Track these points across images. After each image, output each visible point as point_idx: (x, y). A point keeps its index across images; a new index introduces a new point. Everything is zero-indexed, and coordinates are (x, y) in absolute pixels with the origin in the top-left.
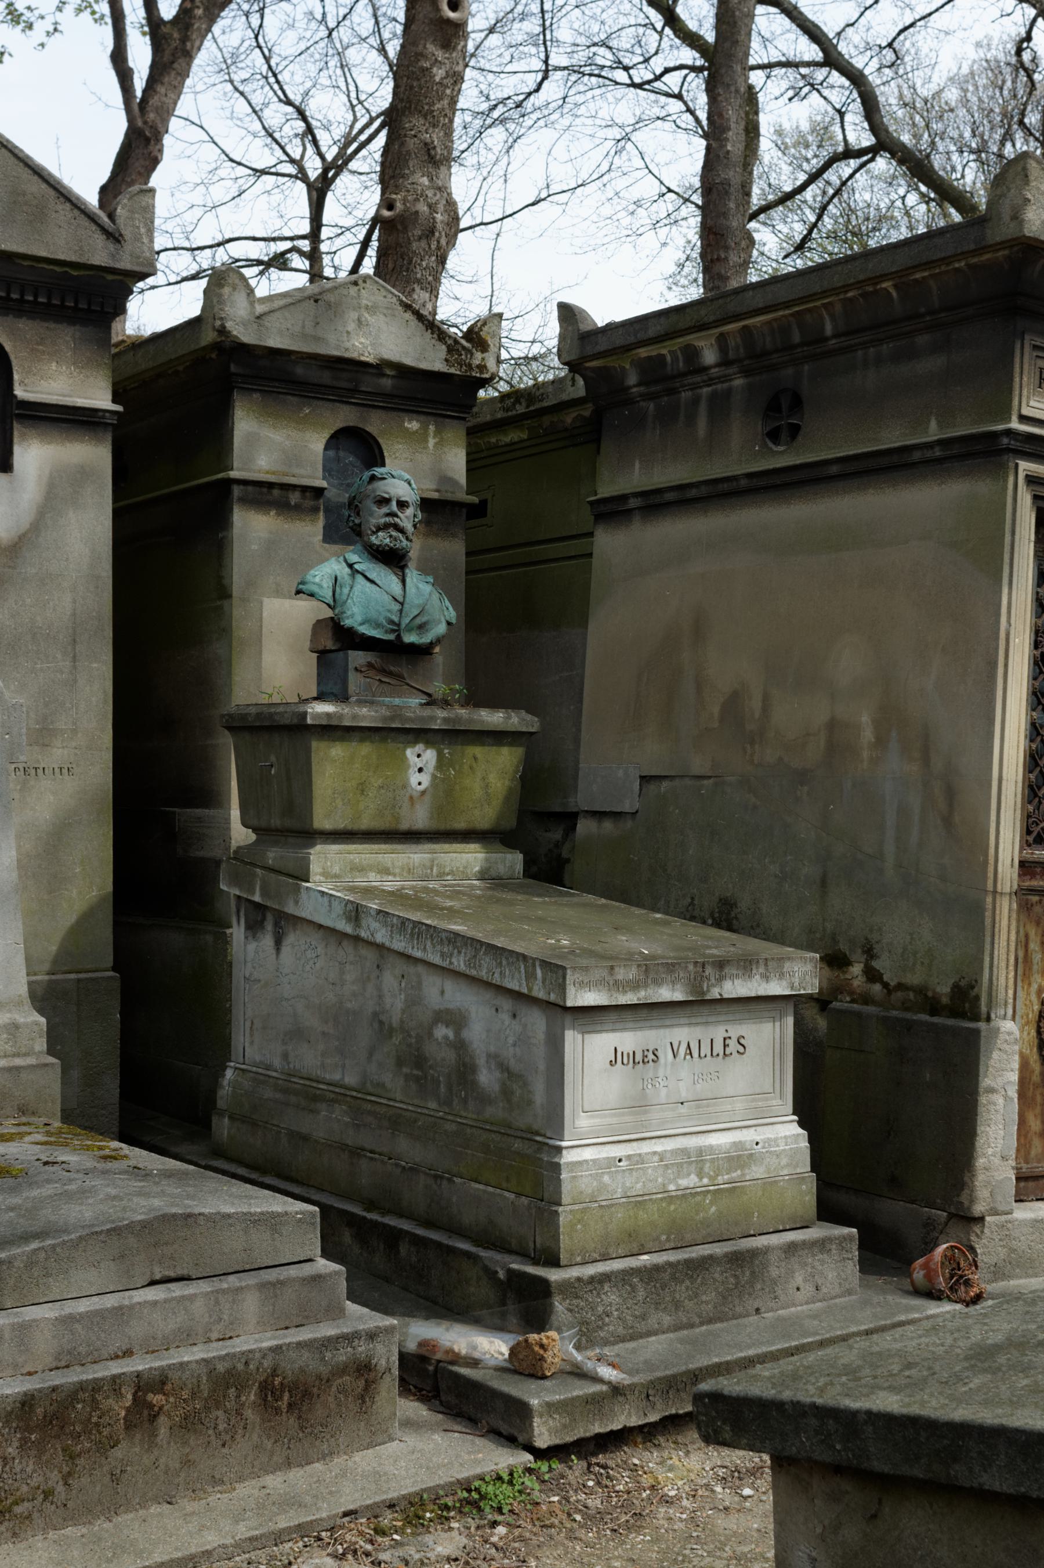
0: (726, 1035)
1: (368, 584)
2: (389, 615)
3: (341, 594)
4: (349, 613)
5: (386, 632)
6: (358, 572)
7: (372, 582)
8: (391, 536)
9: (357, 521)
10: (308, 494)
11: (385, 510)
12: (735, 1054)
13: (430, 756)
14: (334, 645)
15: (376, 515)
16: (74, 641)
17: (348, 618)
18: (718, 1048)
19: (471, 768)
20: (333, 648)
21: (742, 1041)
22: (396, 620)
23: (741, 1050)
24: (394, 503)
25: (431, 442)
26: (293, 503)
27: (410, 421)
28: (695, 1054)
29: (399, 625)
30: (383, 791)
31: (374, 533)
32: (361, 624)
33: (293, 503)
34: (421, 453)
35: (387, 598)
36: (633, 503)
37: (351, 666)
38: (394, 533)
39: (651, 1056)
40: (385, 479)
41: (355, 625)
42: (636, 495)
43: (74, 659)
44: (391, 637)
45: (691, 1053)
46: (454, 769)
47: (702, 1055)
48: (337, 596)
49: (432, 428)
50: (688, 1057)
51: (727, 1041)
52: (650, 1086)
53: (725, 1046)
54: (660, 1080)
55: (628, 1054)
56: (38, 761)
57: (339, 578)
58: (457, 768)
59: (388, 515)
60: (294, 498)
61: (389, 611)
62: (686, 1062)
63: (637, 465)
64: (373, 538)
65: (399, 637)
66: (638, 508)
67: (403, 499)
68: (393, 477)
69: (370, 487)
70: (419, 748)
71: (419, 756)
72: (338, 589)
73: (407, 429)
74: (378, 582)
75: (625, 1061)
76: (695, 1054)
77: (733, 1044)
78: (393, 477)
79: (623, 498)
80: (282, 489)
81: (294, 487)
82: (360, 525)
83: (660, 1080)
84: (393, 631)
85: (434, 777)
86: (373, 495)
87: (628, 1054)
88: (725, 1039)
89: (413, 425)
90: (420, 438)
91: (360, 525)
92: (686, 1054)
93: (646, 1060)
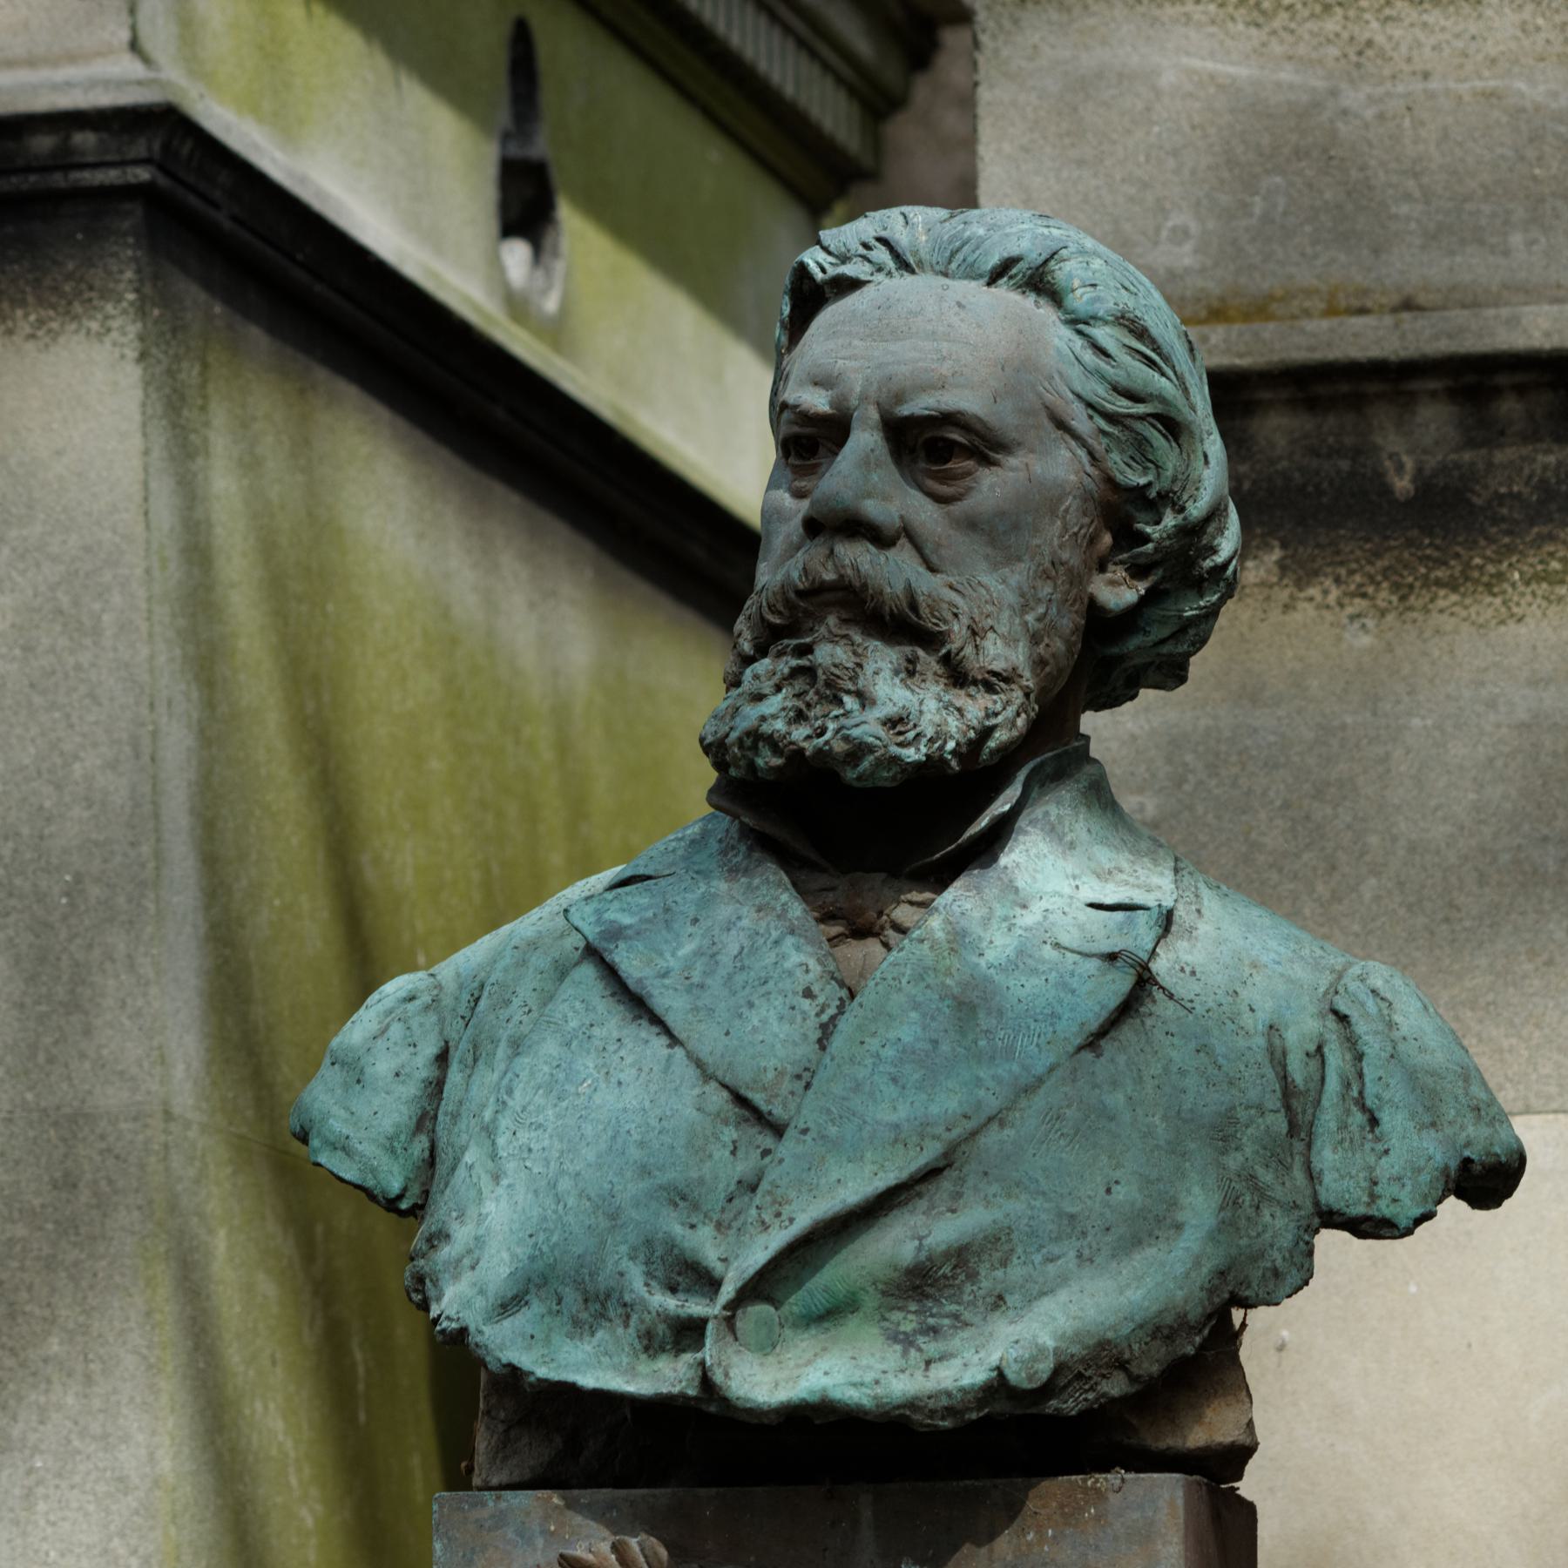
2: (674, 1226)
4: (462, 1235)
5: (651, 1344)
7: (637, 1004)
10: (1509, 407)
24: (865, 439)
26: (1403, 485)
32: (508, 1306)
33: (1403, 485)
40: (853, 284)
41: (472, 1319)
60: (1411, 446)
61: (681, 1197)
67: (920, 405)
68: (904, 265)
80: (1312, 405)
81: (1394, 379)
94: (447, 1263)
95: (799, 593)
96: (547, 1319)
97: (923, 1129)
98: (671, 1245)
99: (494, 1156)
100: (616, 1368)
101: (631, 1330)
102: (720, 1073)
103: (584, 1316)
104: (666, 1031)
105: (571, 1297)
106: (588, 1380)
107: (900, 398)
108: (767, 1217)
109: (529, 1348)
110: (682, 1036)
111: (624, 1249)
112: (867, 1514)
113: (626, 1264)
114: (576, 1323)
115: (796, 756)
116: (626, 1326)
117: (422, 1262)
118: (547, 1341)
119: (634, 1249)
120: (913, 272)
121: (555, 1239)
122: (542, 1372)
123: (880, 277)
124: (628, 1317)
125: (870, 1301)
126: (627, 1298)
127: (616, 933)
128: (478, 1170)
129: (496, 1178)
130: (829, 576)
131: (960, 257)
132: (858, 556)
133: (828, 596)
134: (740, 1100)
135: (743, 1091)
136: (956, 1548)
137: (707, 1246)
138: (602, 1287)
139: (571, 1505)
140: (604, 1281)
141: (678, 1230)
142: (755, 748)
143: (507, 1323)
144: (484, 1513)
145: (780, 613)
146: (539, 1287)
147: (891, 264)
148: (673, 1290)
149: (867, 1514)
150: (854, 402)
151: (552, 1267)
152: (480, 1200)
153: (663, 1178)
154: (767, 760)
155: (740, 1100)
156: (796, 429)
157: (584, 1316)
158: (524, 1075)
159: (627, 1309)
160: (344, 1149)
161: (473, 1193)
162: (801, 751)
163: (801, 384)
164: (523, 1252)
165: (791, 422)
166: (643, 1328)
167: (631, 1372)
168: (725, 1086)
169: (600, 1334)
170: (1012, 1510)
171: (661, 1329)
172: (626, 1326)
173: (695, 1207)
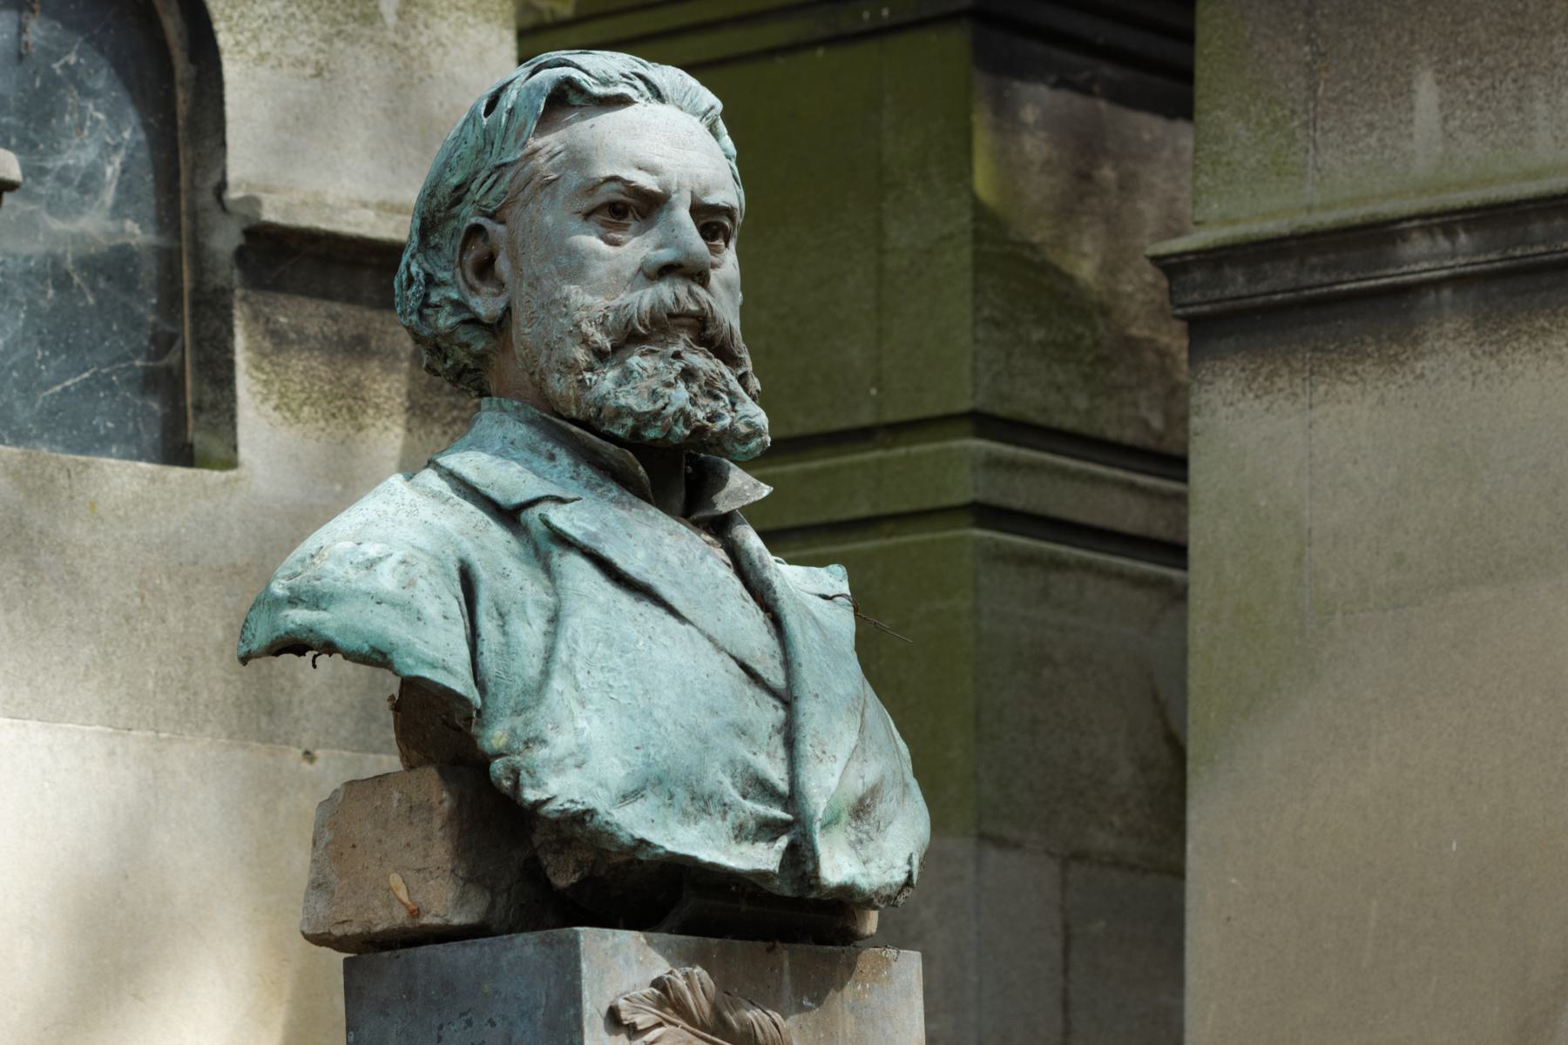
1: (624, 601)
2: (742, 750)
3: (508, 649)
4: (561, 743)
6: (563, 540)
8: (688, 375)
9: (485, 305)
11: (638, 248)
14: (461, 901)
15: (599, 270)
17: (558, 766)
20: (457, 920)
22: (777, 775)
24: (683, 214)
29: (792, 799)
31: (601, 355)
32: (628, 797)
34: (352, 39)
36: (1421, 257)
37: (593, 1008)
38: (701, 361)
40: (622, 101)
42: (1445, 221)
44: (764, 857)
48: (489, 661)
57: (483, 574)
59: (666, 271)
63: (1426, 91)
64: (606, 381)
65: (800, 857)
66: (1458, 281)
68: (658, 95)
69: (551, 141)
72: (487, 625)
74: (667, 592)
78: (658, 95)
79: (1376, 235)
82: (499, 327)
84: (768, 830)
86: (574, 179)
91: (499, 327)
94: (547, 762)
95: (671, 315)
96: (662, 809)
98: (748, 766)
99: (577, 688)
100: (718, 848)
101: (728, 823)
102: (727, 647)
103: (691, 809)
104: (672, 611)
105: (682, 795)
106: (706, 855)
107: (706, 192)
108: (819, 753)
109: (652, 829)
110: (690, 618)
111: (717, 764)
112: (786, 964)
113: (721, 776)
114: (685, 814)
115: (700, 431)
116: (724, 819)
117: (518, 758)
118: (665, 826)
119: (724, 765)
120: (663, 102)
121: (665, 752)
122: (670, 847)
123: (642, 101)
124: (725, 813)
125: (845, 817)
126: (727, 800)
127: (595, 537)
128: (567, 696)
129: (582, 704)
130: (693, 307)
131: (688, 98)
133: (685, 321)
134: (744, 667)
135: (748, 662)
136: (827, 992)
138: (707, 791)
139: (650, 943)
140: (708, 785)
141: (750, 756)
142: (676, 421)
143: (629, 809)
144: (608, 944)
145: (645, 326)
146: (654, 786)
147: (648, 94)
148: (744, 797)
149: (786, 964)
150: (674, 188)
151: (667, 772)
152: (572, 718)
153: (731, 716)
154: (681, 430)
155: (744, 667)
156: (622, 197)
157: (691, 809)
158: (580, 629)
159: (725, 807)
160: (444, 668)
161: (565, 713)
162: (703, 429)
163: (623, 166)
164: (638, 759)
165: (618, 191)
166: (737, 822)
167: (726, 852)
168: (733, 657)
169: (702, 824)
170: (851, 967)
171: (751, 824)
172: (724, 819)
173: (753, 740)
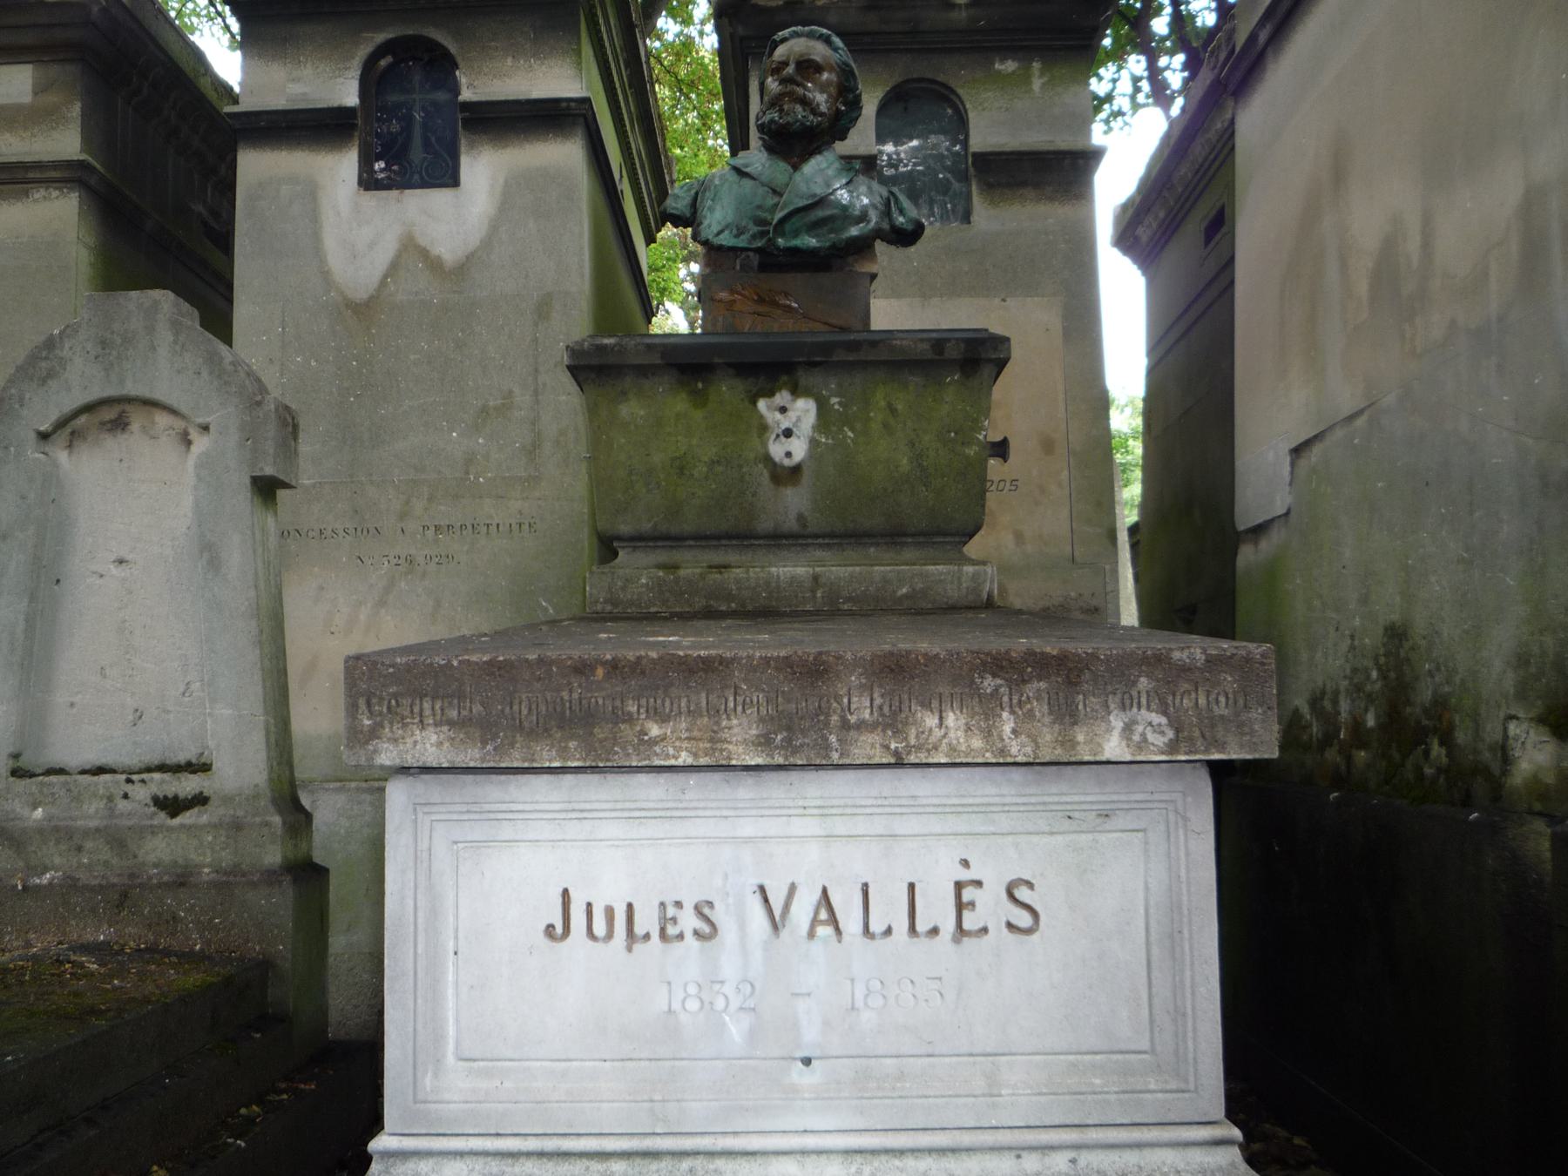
0: (965, 875)
12: (998, 932)
13: (804, 411)
16: (536, 370)
18: (937, 909)
19: (886, 426)
21: (1023, 894)
23: (1024, 920)
25: (1037, 84)
27: (1002, 61)
28: (851, 921)
30: (719, 469)
35: (761, 191)
39: (688, 921)
43: (536, 393)
45: (833, 921)
46: (852, 429)
47: (876, 926)
49: (1036, 65)
50: (824, 931)
51: (968, 894)
52: (693, 1005)
53: (960, 906)
54: (728, 989)
55: (610, 913)
56: (491, 517)
58: (858, 426)
62: (816, 948)
65: (771, 242)
70: (782, 397)
71: (783, 410)
73: (999, 72)
75: (600, 928)
76: (851, 921)
77: (989, 907)
83: (728, 989)
85: (813, 443)
87: (610, 913)
88: (959, 886)
89: (1010, 66)
90: (1024, 79)
92: (815, 922)
93: (672, 930)
97: (815, 195)
132: (790, 88)
137: (767, 216)
